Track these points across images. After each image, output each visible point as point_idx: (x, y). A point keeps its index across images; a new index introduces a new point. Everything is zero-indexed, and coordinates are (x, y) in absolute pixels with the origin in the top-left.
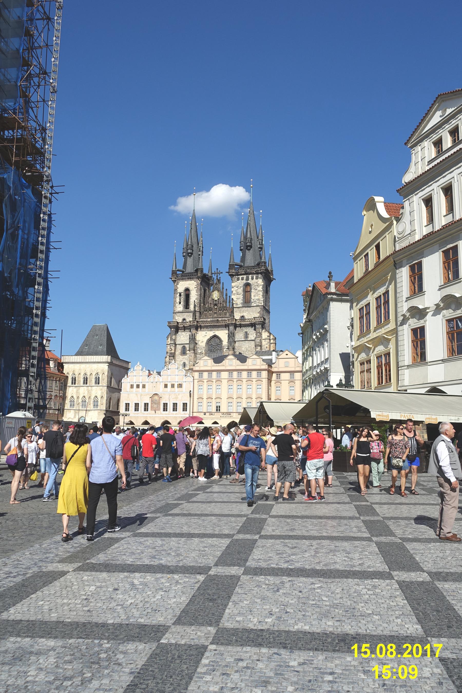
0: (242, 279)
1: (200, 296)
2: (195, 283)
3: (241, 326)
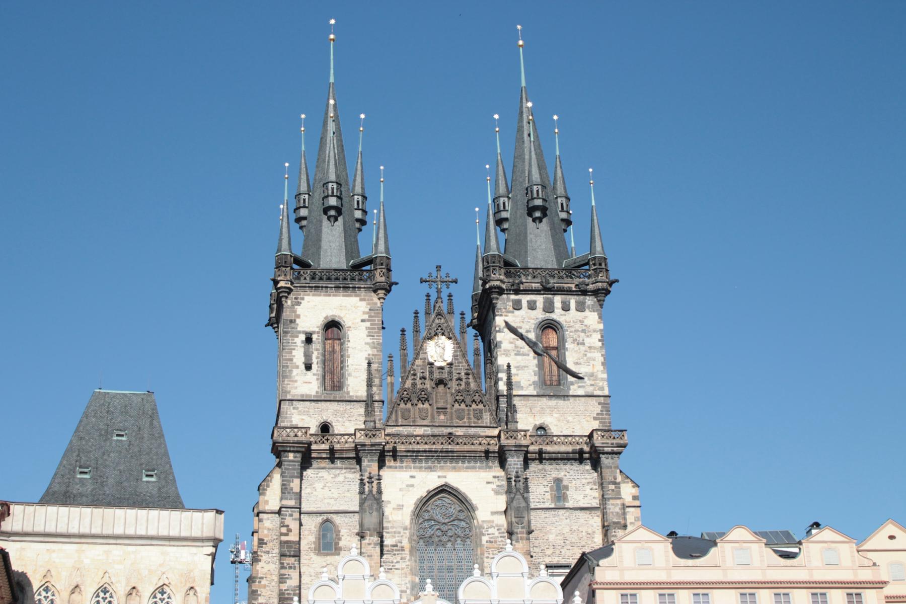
0: (532, 306)
2: (363, 306)
3: (541, 457)
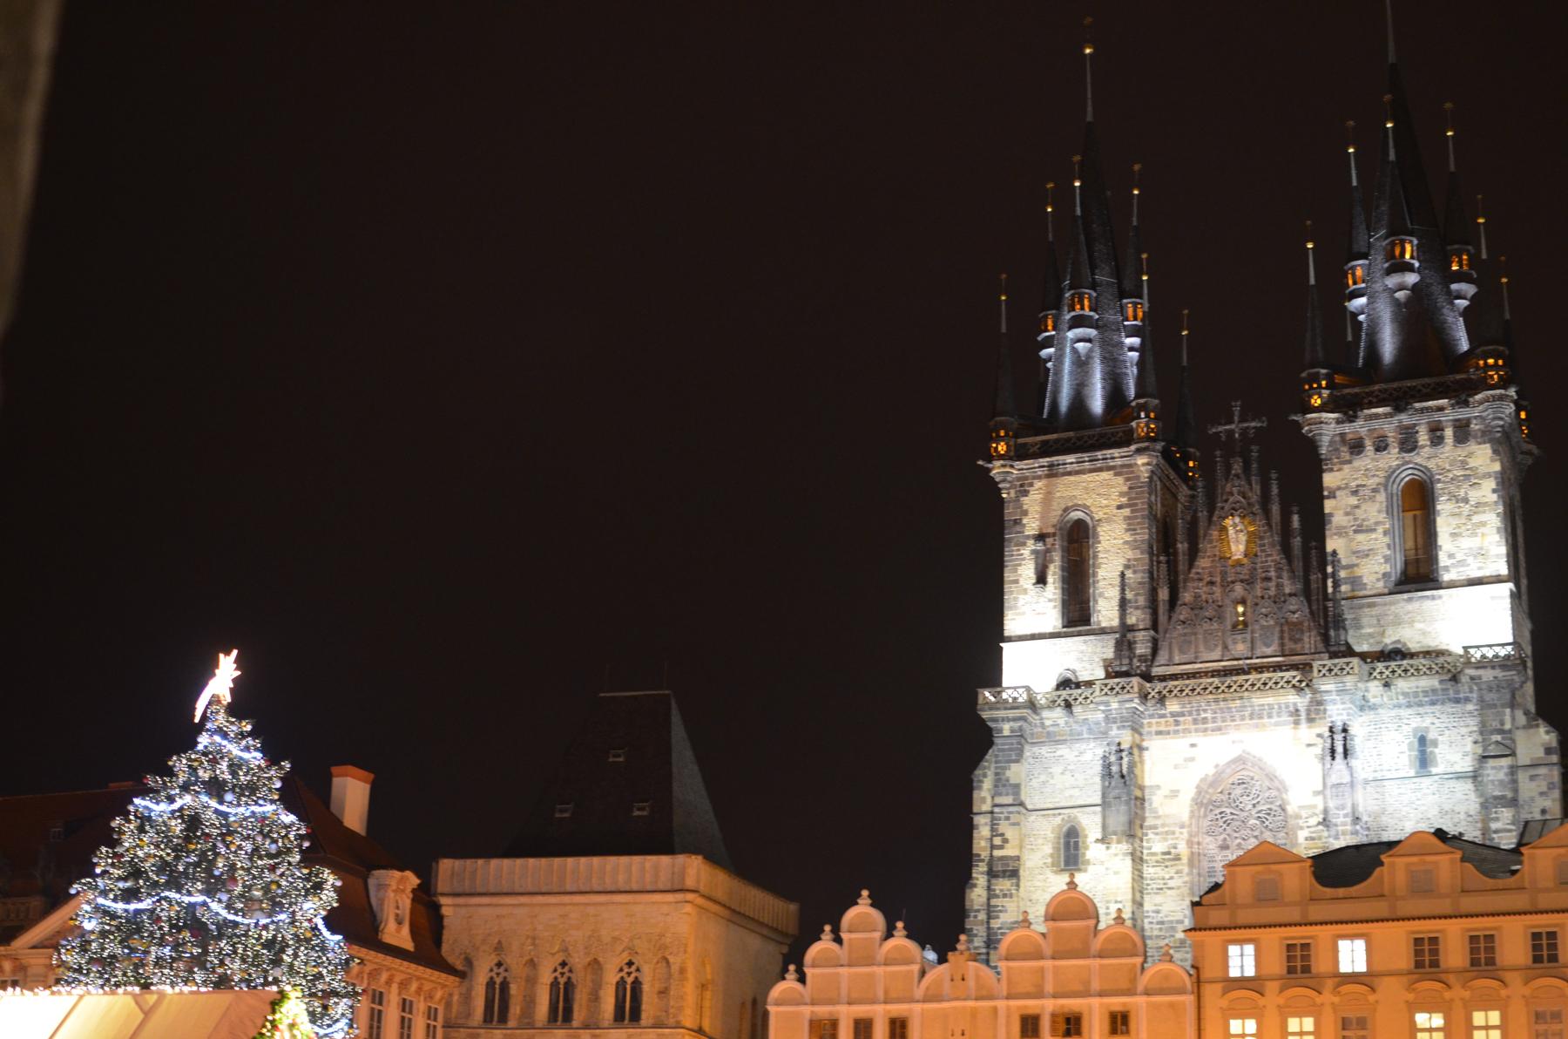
0: (1381, 446)
1: (1151, 554)
